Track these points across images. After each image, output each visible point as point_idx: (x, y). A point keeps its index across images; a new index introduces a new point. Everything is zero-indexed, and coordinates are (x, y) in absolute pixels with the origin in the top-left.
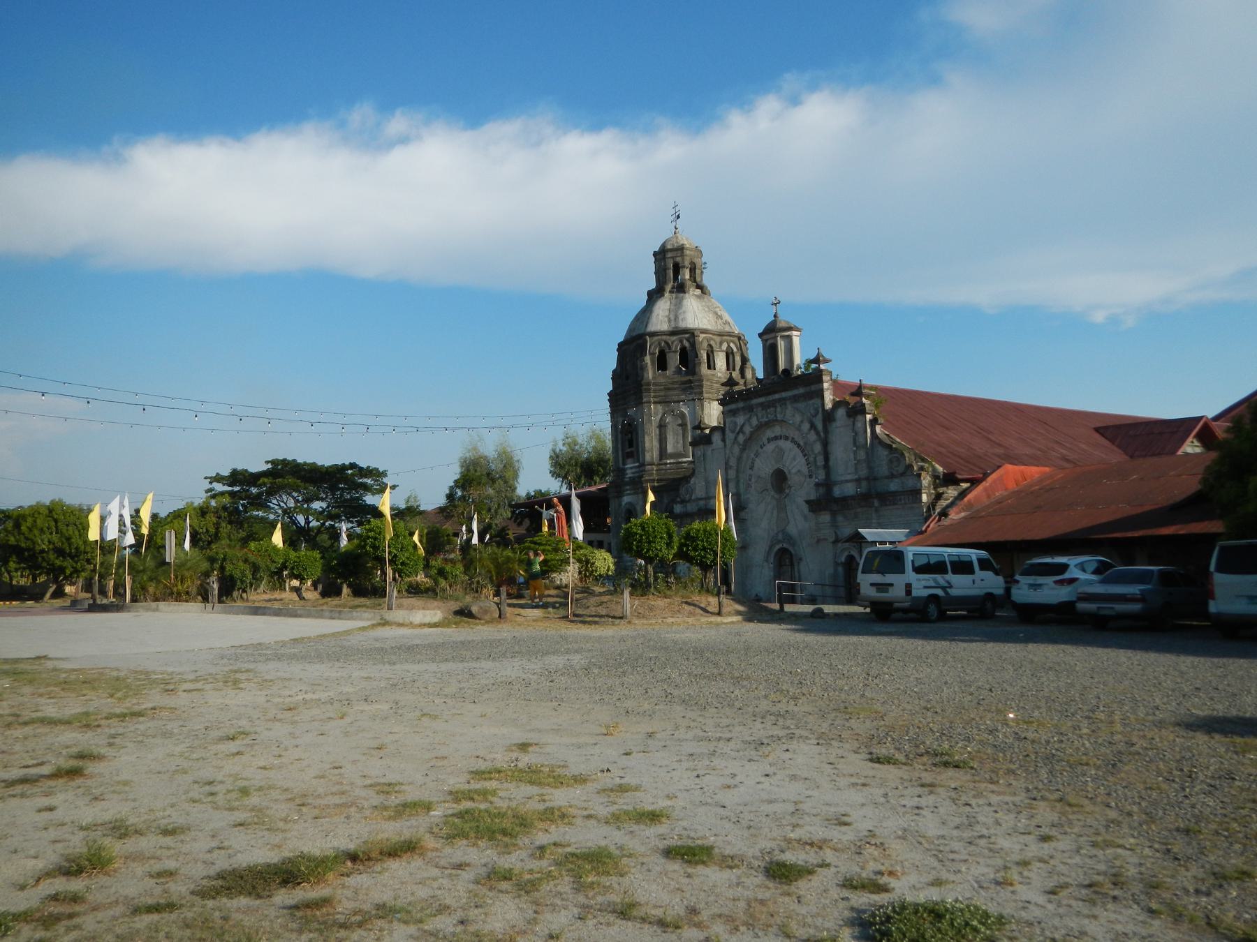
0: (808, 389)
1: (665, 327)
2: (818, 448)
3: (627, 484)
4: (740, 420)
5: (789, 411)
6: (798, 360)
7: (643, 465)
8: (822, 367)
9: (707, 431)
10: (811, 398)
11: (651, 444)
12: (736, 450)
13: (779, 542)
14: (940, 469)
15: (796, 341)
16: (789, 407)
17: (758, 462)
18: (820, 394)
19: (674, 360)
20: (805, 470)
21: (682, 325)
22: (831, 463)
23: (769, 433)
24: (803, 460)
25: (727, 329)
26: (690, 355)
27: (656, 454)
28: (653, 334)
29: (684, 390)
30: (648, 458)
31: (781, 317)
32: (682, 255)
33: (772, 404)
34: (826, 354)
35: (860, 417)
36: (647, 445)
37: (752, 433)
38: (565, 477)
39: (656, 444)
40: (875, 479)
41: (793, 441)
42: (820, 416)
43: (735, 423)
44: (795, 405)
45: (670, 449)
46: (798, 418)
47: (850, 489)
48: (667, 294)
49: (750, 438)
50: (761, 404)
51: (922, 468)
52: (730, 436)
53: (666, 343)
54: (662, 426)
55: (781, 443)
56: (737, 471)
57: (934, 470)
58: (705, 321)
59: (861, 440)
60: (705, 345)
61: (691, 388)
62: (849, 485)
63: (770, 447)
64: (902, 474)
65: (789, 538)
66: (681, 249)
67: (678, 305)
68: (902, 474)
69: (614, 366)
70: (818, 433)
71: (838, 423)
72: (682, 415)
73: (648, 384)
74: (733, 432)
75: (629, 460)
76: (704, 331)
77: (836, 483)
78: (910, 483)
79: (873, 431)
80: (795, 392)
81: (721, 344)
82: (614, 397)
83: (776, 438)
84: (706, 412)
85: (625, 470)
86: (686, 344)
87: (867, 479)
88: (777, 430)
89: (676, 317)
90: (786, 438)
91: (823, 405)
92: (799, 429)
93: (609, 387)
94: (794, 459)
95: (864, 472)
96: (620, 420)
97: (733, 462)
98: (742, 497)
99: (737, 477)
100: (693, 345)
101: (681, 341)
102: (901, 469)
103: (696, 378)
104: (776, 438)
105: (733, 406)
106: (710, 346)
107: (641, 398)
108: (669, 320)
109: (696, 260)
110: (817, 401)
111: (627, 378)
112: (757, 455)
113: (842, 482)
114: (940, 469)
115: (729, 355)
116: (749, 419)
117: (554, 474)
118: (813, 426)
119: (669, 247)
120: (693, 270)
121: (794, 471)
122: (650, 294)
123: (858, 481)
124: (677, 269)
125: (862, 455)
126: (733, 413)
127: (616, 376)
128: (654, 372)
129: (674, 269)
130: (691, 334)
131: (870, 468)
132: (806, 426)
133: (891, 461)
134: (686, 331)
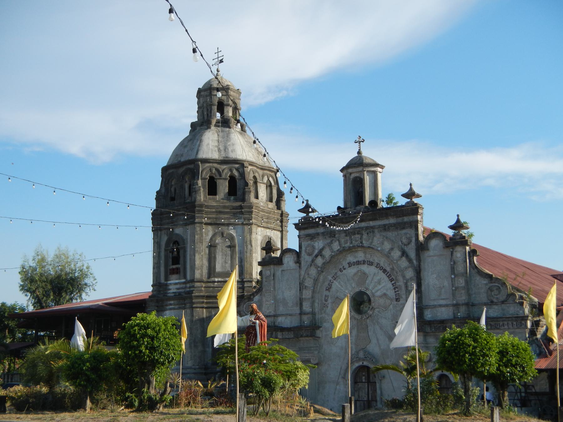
0: (400, 220)
1: (215, 156)
2: (410, 273)
3: (170, 299)
4: (319, 244)
5: (377, 240)
6: (382, 195)
7: (193, 281)
8: (415, 200)
9: (278, 254)
10: (404, 228)
11: (200, 261)
12: (313, 272)
13: (359, 359)
14: (536, 300)
15: (379, 175)
16: (378, 235)
18: (414, 225)
19: (223, 187)
21: (232, 156)
22: (423, 288)
23: (351, 258)
24: (390, 285)
25: (267, 164)
26: (239, 184)
27: (205, 271)
28: (205, 161)
29: (235, 215)
30: (197, 275)
31: (364, 154)
32: (228, 95)
34: (416, 190)
35: (459, 249)
36: (198, 262)
37: (332, 257)
38: (33, 292)
39: (206, 263)
40: (473, 305)
41: (378, 266)
42: (413, 244)
43: (313, 247)
44: (384, 234)
45: (218, 268)
46: (387, 246)
47: (444, 313)
48: (213, 127)
49: (328, 263)
51: (521, 297)
52: (306, 258)
53: (217, 170)
54: (212, 247)
56: (314, 292)
57: (530, 299)
58: (250, 154)
59: (460, 268)
60: (251, 175)
61: (242, 213)
62: (443, 309)
63: (352, 271)
64: (503, 302)
65: (369, 356)
66: (226, 89)
67: (227, 137)
68: (503, 302)
69: (158, 188)
70: (410, 260)
71: (431, 253)
72: (231, 238)
73: (201, 206)
74: (309, 255)
75: (174, 276)
76: (251, 164)
77: (428, 307)
78: (512, 310)
79: (471, 262)
80: (385, 222)
81: (263, 176)
82: (159, 218)
83: (358, 263)
84: (254, 236)
85: (166, 285)
86: (236, 173)
87: (467, 304)
88: (360, 256)
89: (226, 149)
90: (371, 264)
91: (417, 235)
92: (388, 256)
93: (153, 205)
94: (379, 282)
95: (462, 298)
96: (165, 238)
97: (309, 283)
98: (318, 316)
99: (312, 297)
100: (242, 175)
101: (231, 170)
102: (502, 297)
103: (245, 204)
104: (358, 263)
105: (311, 231)
106: (255, 177)
107: (194, 217)
108: (219, 150)
109: (237, 101)
110: (412, 232)
111: (173, 199)
112: (335, 277)
113: (435, 306)
114: (536, 300)
115: (269, 186)
116: (330, 244)
117: (23, 288)
118: (404, 253)
119: (215, 85)
120: (236, 109)
121: (379, 294)
122: (193, 125)
123: (456, 306)
124: (221, 107)
125: (461, 282)
126: (312, 237)
127: (159, 196)
128: (205, 196)
129: (216, 105)
130: (241, 164)
131: (469, 295)
132: (396, 254)
133: (490, 289)
134: (236, 161)
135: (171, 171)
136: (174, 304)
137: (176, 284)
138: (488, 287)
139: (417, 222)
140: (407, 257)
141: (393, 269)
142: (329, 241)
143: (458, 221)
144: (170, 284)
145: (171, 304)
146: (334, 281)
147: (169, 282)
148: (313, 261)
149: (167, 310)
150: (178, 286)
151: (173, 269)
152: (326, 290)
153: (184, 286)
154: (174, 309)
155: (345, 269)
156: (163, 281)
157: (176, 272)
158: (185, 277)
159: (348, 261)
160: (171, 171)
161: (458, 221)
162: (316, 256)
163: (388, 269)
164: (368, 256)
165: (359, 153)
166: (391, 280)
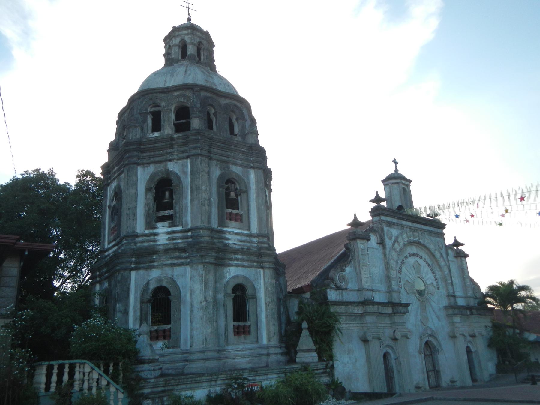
10: (438, 237)
17: (404, 269)
20: (435, 284)
50: (410, 227)
55: (418, 259)
75: (234, 223)
83: (414, 255)
90: (421, 258)
94: (427, 273)
104: (414, 255)
116: (402, 234)
118: (441, 255)
135: (208, 94)
136: (243, 260)
137: (237, 234)
139: (444, 234)
141: (432, 264)
142: (400, 232)
143: (456, 241)
144: (229, 232)
145: (237, 259)
147: (225, 229)
148: (393, 245)
149: (232, 265)
150: (239, 237)
151: (231, 214)
153: (248, 238)
154: (244, 266)
156: (215, 224)
157: (238, 218)
158: (249, 229)
159: (408, 252)
160: (208, 94)
161: (456, 241)
162: (395, 241)
163: (430, 263)
165: (396, 171)
166: (433, 273)
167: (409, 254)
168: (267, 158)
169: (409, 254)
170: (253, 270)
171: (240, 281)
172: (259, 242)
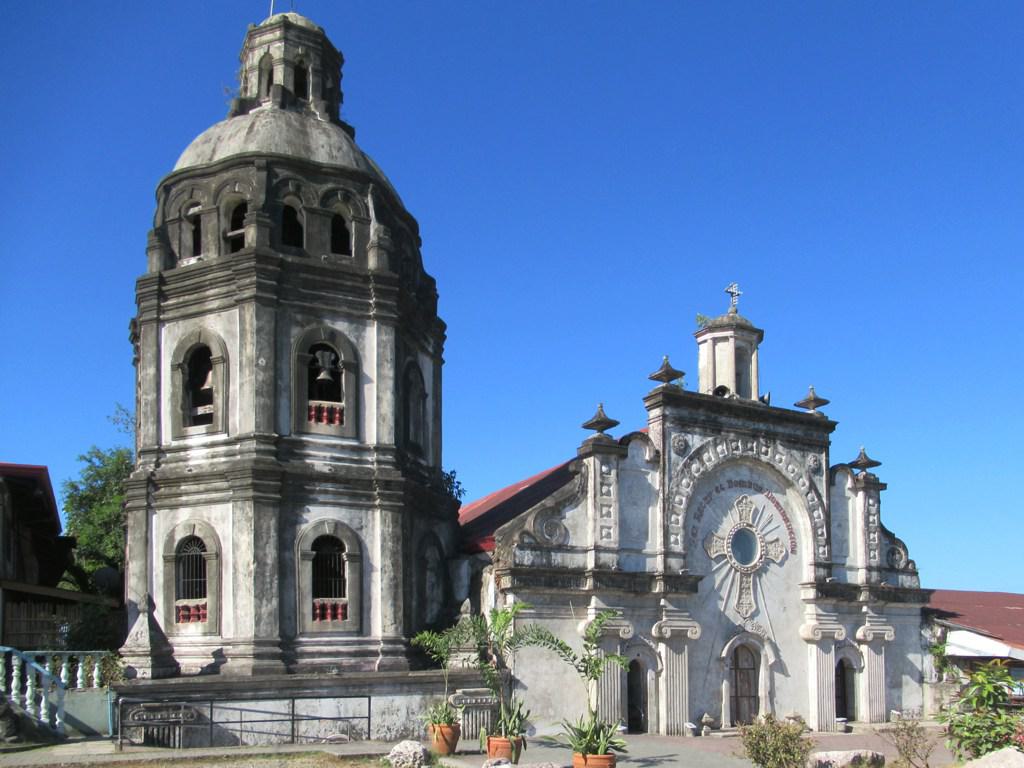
18: (824, 446)
33: (755, 436)
136: (335, 493)
138: (888, 549)
140: (817, 491)
145: (326, 492)
146: (708, 506)
152: (695, 517)
155: (723, 489)
158: (358, 433)
164: (755, 477)
167: (730, 482)
168: (438, 296)
169: (730, 482)
170: (354, 512)
171: (327, 530)
172: (379, 462)
